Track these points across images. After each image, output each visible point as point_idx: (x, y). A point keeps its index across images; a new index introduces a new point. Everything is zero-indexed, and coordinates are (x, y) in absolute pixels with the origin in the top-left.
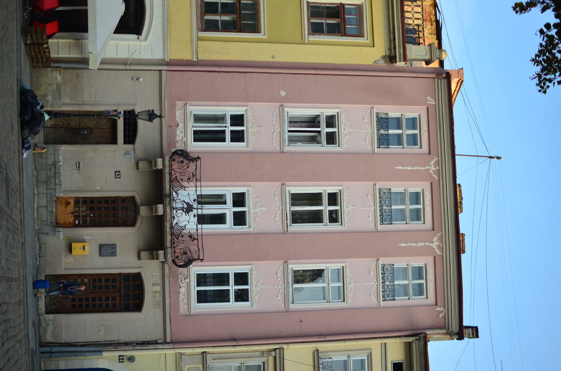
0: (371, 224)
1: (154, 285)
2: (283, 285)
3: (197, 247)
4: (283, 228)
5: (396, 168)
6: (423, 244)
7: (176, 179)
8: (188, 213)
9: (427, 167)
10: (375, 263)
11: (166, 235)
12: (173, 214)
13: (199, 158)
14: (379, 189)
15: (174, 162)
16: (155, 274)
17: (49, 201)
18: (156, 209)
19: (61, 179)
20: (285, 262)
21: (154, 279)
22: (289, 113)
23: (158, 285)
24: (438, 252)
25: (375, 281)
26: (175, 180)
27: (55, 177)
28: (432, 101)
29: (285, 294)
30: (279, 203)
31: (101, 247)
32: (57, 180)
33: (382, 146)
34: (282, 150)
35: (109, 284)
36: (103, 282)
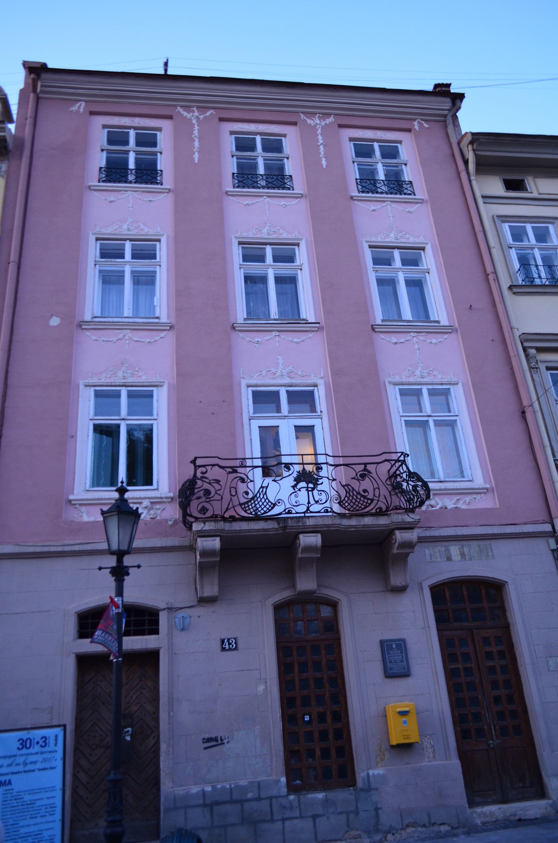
0: (293, 203)
1: (449, 559)
2: (412, 334)
3: (380, 465)
4: (313, 331)
5: (196, 161)
6: (320, 137)
7: (246, 505)
8: (317, 480)
9: (194, 121)
10: (356, 202)
11: (364, 526)
12: (319, 512)
13: (194, 462)
14: (234, 188)
15: (207, 510)
16: (428, 558)
17: (300, 814)
18: (308, 549)
19: (246, 783)
20: (373, 329)
21: (439, 559)
22: (95, 315)
23: (449, 551)
24: (331, 119)
25: (385, 204)
26: (248, 506)
27: (241, 802)
28: (80, 106)
29: (427, 332)
30: (267, 336)
31: (389, 675)
32: (250, 795)
33: (159, 178)
34: (168, 328)
35: (459, 653)
36: (457, 666)
